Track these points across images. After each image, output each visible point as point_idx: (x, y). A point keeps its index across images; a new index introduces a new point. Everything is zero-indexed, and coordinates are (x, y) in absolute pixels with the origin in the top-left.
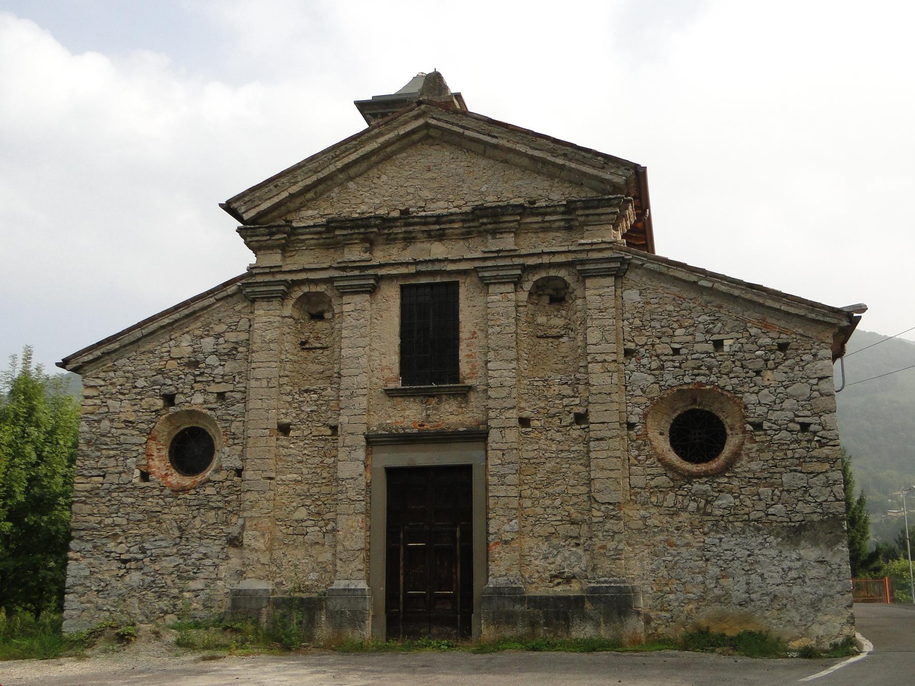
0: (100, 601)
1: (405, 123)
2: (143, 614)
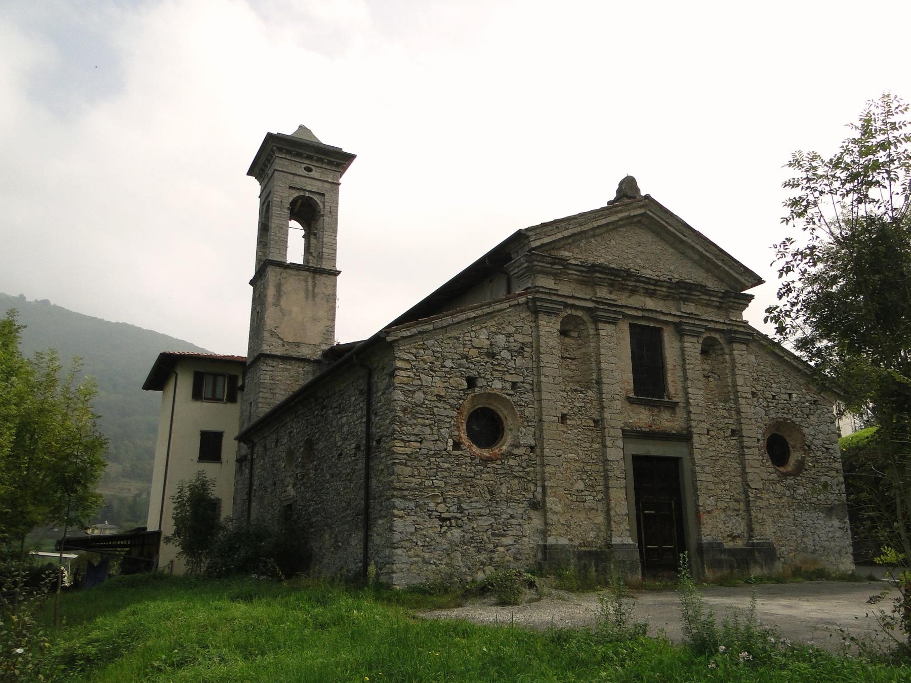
0: (427, 556)
1: (635, 208)
2: (466, 566)
